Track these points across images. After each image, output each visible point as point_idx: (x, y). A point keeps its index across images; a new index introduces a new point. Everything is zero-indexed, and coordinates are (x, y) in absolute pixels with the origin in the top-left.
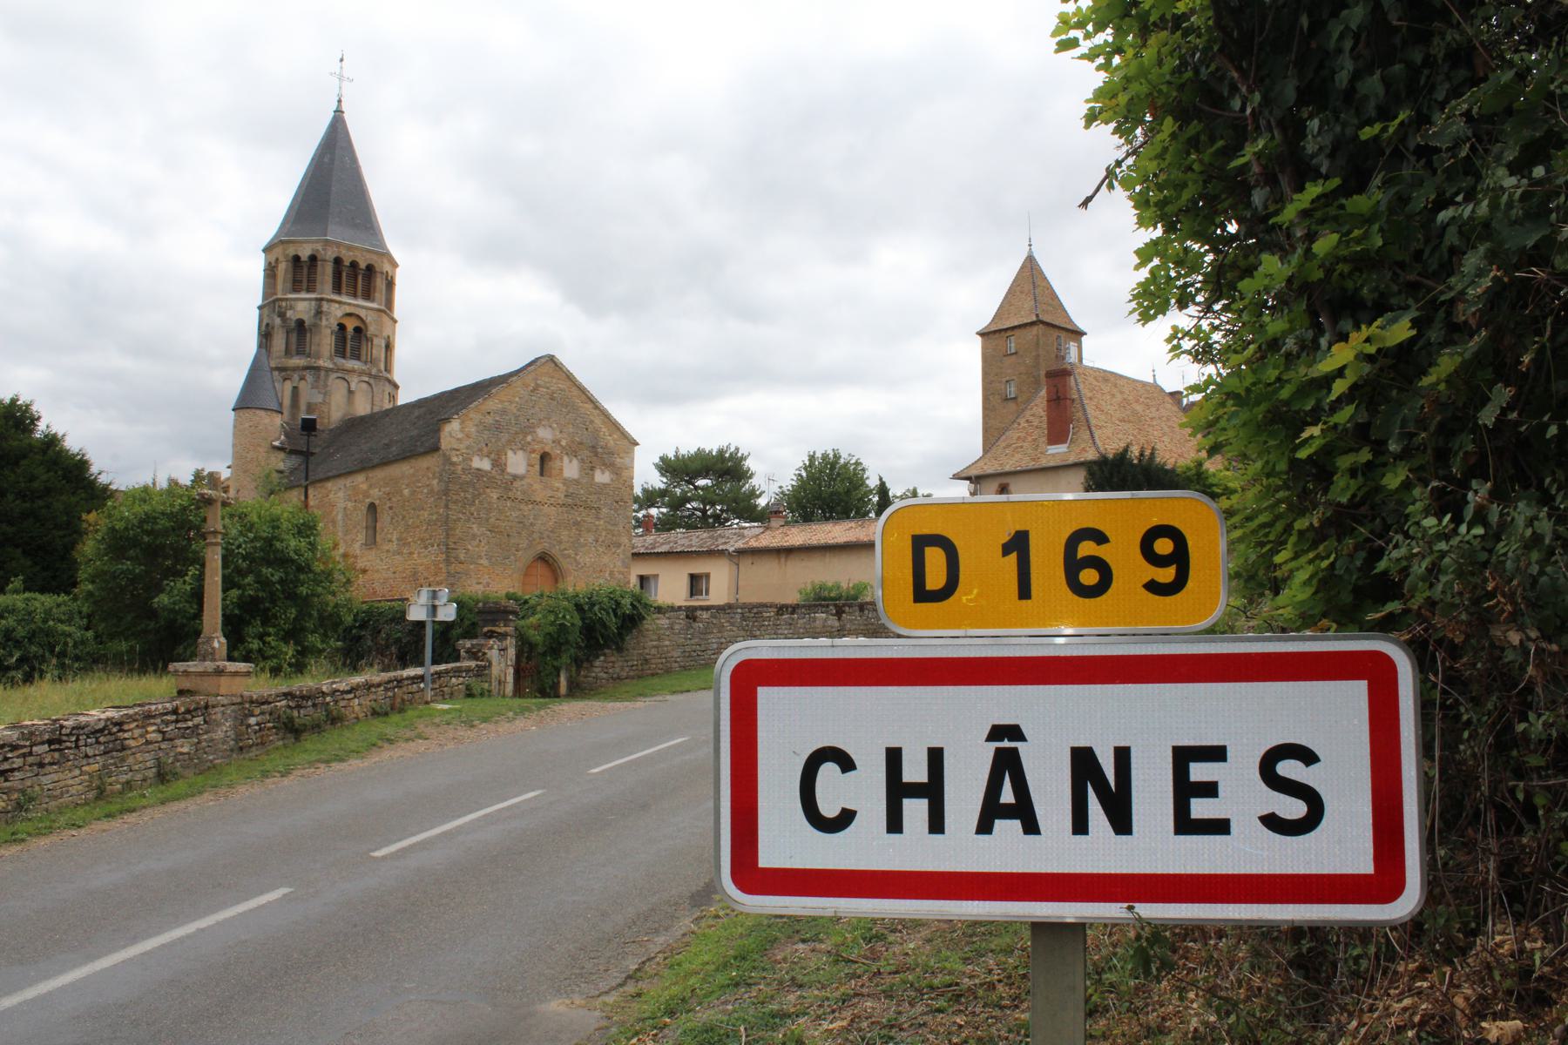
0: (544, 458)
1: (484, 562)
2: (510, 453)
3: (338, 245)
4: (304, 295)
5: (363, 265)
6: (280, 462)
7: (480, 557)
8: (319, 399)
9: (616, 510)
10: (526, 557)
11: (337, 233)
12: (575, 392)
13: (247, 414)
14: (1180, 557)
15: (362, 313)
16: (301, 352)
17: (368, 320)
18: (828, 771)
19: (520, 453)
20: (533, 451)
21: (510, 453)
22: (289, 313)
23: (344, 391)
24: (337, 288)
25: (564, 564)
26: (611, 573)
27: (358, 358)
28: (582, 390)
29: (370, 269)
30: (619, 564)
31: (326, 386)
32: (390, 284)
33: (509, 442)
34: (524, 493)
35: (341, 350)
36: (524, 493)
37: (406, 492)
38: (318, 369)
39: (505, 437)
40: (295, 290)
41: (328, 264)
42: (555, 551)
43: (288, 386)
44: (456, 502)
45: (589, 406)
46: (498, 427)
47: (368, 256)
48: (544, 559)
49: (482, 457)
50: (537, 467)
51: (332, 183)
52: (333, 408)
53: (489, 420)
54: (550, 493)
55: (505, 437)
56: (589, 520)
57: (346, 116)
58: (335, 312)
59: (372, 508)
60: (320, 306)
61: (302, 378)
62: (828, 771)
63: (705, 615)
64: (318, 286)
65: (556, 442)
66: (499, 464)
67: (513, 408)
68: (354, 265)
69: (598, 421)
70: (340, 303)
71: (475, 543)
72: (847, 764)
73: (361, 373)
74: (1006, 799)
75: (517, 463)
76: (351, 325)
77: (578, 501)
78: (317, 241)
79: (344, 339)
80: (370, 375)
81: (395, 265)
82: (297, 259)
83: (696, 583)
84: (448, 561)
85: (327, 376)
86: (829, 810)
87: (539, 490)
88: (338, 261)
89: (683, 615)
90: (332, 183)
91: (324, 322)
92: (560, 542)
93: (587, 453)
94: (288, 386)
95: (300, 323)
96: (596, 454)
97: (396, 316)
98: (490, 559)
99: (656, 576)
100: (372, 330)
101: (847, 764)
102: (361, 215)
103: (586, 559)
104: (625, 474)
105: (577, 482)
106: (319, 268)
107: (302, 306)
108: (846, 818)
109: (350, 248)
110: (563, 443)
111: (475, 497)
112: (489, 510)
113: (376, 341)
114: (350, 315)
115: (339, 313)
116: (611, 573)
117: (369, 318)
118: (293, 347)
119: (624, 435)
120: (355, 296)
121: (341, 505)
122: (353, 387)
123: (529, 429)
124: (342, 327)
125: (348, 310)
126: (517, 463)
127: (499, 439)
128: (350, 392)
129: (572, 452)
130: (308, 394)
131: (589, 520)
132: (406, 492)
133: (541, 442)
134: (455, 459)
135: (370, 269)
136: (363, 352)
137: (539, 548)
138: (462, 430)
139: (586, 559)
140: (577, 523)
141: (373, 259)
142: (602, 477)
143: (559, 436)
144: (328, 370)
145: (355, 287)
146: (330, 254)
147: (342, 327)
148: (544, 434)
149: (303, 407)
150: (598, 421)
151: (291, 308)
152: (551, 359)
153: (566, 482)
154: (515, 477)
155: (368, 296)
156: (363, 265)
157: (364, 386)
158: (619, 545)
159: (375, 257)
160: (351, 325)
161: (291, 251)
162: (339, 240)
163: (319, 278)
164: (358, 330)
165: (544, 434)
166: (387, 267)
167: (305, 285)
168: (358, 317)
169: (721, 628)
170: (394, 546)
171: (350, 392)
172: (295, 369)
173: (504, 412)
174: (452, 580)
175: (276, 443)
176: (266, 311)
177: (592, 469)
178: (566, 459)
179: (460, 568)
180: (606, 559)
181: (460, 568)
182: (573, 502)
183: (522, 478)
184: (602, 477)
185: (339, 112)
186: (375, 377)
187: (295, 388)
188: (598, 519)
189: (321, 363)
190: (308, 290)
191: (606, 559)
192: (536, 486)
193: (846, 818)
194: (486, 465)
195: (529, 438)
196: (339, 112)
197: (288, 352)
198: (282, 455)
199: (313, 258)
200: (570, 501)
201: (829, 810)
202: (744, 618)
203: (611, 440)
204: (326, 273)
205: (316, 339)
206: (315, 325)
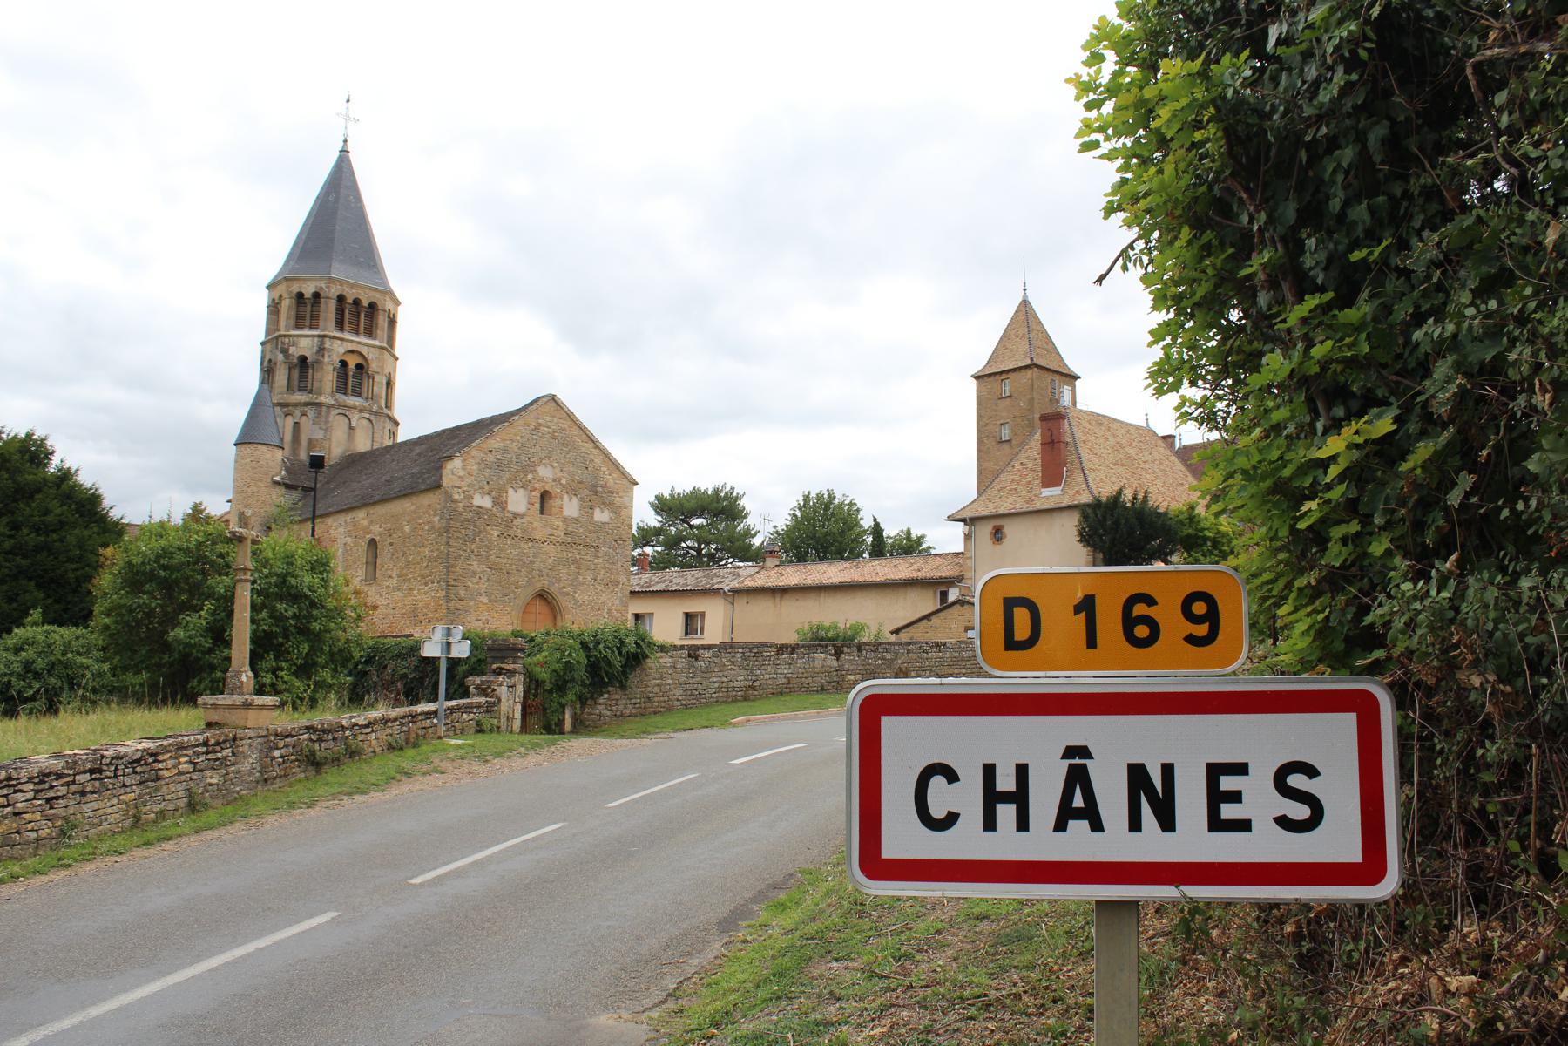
0: (545, 496)
1: (484, 599)
2: (511, 491)
3: (342, 282)
4: (306, 332)
5: (365, 303)
6: (280, 497)
8: (319, 434)
9: (615, 549)
10: (526, 594)
11: (339, 271)
12: (576, 431)
13: (248, 449)
14: (1212, 617)
15: (364, 350)
16: (303, 386)
17: (370, 357)
18: (937, 782)
20: (534, 490)
21: (511, 491)
22: (292, 350)
23: (346, 428)
24: (340, 325)
25: (564, 602)
26: (610, 611)
27: (359, 395)
28: (583, 429)
29: (372, 306)
31: (327, 422)
32: (392, 322)
33: (510, 480)
34: (524, 531)
35: (342, 387)
36: (524, 531)
37: (407, 529)
38: (319, 405)
39: (506, 475)
40: (298, 326)
42: (554, 589)
43: (290, 421)
44: (457, 539)
45: (590, 445)
46: (499, 465)
47: (372, 294)
48: (543, 596)
49: (483, 494)
50: (538, 505)
51: (336, 222)
52: (334, 443)
53: (491, 458)
55: (506, 475)
57: (352, 156)
58: (337, 349)
59: (373, 542)
60: (322, 343)
61: (304, 414)
62: (937, 782)
63: (707, 654)
64: (321, 323)
65: (557, 480)
66: (500, 502)
68: (357, 302)
69: (598, 461)
72: (951, 776)
73: (362, 410)
74: (1077, 806)
75: (518, 501)
76: (352, 362)
77: (578, 540)
78: (321, 279)
79: (346, 376)
80: (371, 412)
81: (397, 303)
82: (300, 296)
83: (691, 622)
84: (447, 597)
85: (328, 412)
86: (938, 812)
87: (539, 527)
89: (685, 654)
90: (336, 222)
91: (326, 359)
94: (290, 421)
95: (303, 359)
97: (397, 352)
99: (703, 614)
100: (373, 367)
101: (951, 776)
102: (366, 254)
103: (584, 597)
104: (624, 513)
105: (576, 520)
106: (322, 306)
107: (305, 344)
108: (952, 819)
109: (352, 286)
110: (564, 482)
111: (476, 534)
112: (489, 548)
113: (377, 378)
114: (352, 352)
115: (342, 350)
116: (610, 611)
117: (371, 355)
118: (296, 383)
119: (624, 475)
120: (357, 333)
121: (341, 540)
122: (354, 423)
123: (530, 467)
124: (344, 364)
125: (351, 347)
126: (518, 501)
127: (500, 478)
128: (351, 428)
129: (572, 491)
130: (309, 430)
132: (407, 529)
133: (542, 480)
134: (456, 497)
135: (372, 306)
136: (365, 389)
137: (539, 586)
138: (464, 468)
139: (584, 597)
140: (575, 561)
141: (376, 297)
142: (601, 516)
143: (559, 474)
144: (330, 407)
145: (358, 324)
146: (334, 291)
147: (344, 364)
148: (544, 472)
149: (304, 442)
150: (598, 461)
151: (294, 344)
152: (553, 398)
153: (566, 520)
154: (516, 515)
155: (370, 333)
156: (365, 303)
159: (377, 295)
160: (352, 362)
161: (295, 288)
162: (342, 278)
163: (322, 315)
164: (359, 367)
165: (544, 472)
166: (389, 305)
167: (308, 322)
168: (361, 354)
169: (722, 667)
170: (394, 583)
171: (351, 428)
172: (296, 405)
173: (506, 450)
174: (451, 616)
175: (277, 479)
176: (268, 347)
177: (592, 507)
178: (566, 497)
179: (459, 604)
180: (604, 598)
181: (459, 604)
182: (572, 541)
183: (522, 516)
184: (601, 516)
185: (344, 151)
186: (376, 414)
187: (296, 424)
189: (322, 399)
190: (311, 328)
191: (604, 598)
192: (536, 524)
193: (952, 819)
194: (486, 502)
195: (530, 477)
196: (344, 151)
197: (289, 388)
198: (282, 490)
199: (317, 295)
200: (569, 539)
201: (938, 812)
202: (745, 658)
203: (611, 480)
204: (329, 310)
205: (317, 375)
206: (318, 362)
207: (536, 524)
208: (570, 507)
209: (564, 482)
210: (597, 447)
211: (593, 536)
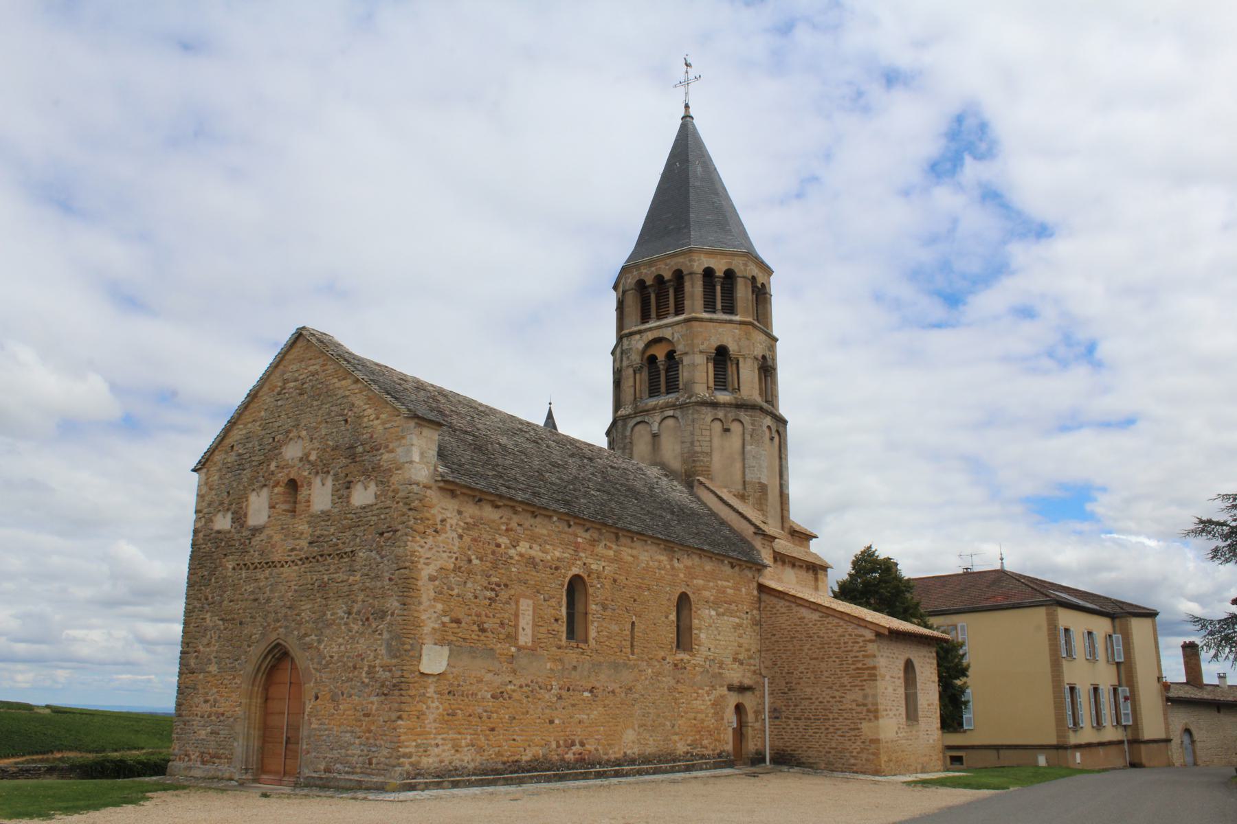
1: (213, 668)
5: (667, 275)
7: (209, 662)
10: (256, 652)
15: (667, 333)
19: (265, 492)
20: (277, 484)
21: (253, 497)
23: (648, 438)
26: (371, 671)
30: (383, 651)
33: (253, 480)
36: (262, 553)
39: (247, 473)
41: (688, 289)
53: (232, 458)
54: (290, 543)
55: (247, 473)
56: (341, 576)
58: (638, 343)
65: (304, 459)
66: (239, 518)
67: (256, 427)
68: (659, 279)
69: (359, 401)
70: (640, 332)
71: (205, 641)
73: (663, 408)
75: (258, 508)
76: (660, 352)
80: (673, 406)
85: (625, 426)
88: (641, 284)
91: (625, 363)
92: (300, 623)
93: (344, 461)
96: (353, 457)
98: (219, 660)
100: (680, 348)
102: (723, 217)
103: (331, 648)
105: (326, 515)
109: (650, 264)
110: (313, 457)
111: (212, 573)
112: (223, 589)
115: (641, 345)
116: (371, 671)
123: (275, 449)
124: (652, 360)
125: (650, 336)
129: (321, 468)
131: (341, 576)
135: (679, 276)
137: (273, 636)
138: (206, 484)
139: (331, 648)
140: (323, 586)
153: (314, 520)
154: (256, 530)
156: (667, 275)
157: (670, 422)
158: (382, 614)
159: (681, 260)
160: (660, 352)
164: (670, 355)
165: (292, 452)
173: (248, 438)
180: (362, 645)
184: (362, 496)
185: (687, 118)
186: (683, 407)
188: (352, 571)
191: (362, 645)
195: (273, 466)
196: (687, 118)
207: (277, 538)
208: (320, 496)
209: (313, 457)
210: (357, 381)
211: (348, 534)
